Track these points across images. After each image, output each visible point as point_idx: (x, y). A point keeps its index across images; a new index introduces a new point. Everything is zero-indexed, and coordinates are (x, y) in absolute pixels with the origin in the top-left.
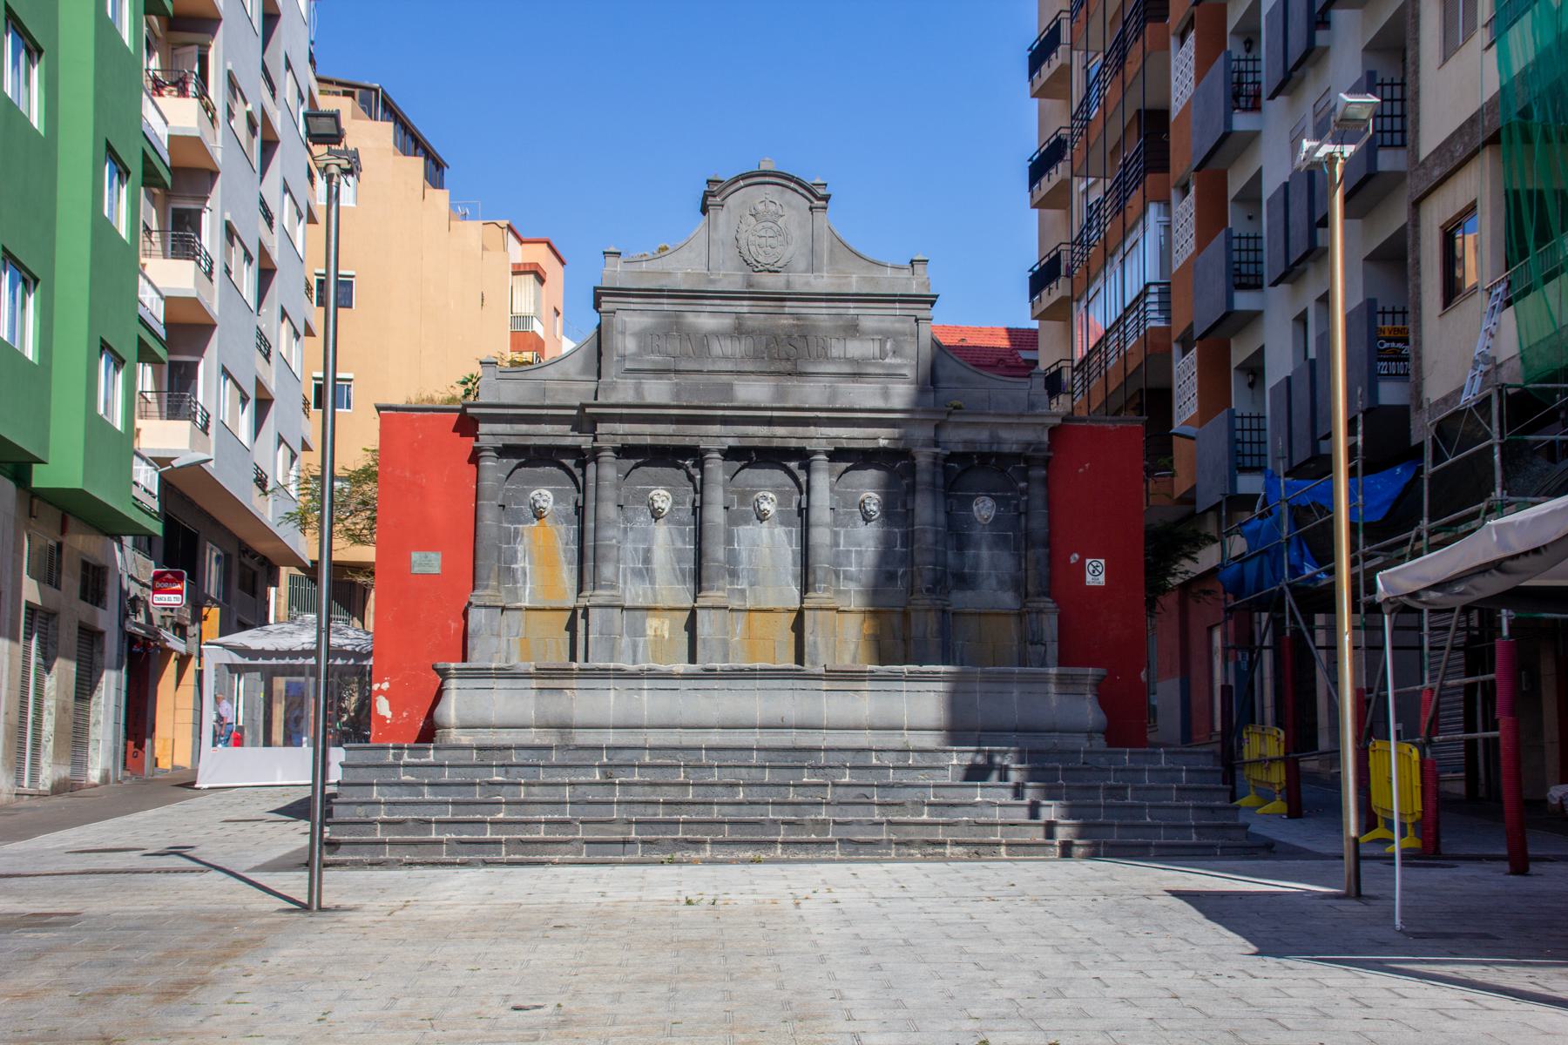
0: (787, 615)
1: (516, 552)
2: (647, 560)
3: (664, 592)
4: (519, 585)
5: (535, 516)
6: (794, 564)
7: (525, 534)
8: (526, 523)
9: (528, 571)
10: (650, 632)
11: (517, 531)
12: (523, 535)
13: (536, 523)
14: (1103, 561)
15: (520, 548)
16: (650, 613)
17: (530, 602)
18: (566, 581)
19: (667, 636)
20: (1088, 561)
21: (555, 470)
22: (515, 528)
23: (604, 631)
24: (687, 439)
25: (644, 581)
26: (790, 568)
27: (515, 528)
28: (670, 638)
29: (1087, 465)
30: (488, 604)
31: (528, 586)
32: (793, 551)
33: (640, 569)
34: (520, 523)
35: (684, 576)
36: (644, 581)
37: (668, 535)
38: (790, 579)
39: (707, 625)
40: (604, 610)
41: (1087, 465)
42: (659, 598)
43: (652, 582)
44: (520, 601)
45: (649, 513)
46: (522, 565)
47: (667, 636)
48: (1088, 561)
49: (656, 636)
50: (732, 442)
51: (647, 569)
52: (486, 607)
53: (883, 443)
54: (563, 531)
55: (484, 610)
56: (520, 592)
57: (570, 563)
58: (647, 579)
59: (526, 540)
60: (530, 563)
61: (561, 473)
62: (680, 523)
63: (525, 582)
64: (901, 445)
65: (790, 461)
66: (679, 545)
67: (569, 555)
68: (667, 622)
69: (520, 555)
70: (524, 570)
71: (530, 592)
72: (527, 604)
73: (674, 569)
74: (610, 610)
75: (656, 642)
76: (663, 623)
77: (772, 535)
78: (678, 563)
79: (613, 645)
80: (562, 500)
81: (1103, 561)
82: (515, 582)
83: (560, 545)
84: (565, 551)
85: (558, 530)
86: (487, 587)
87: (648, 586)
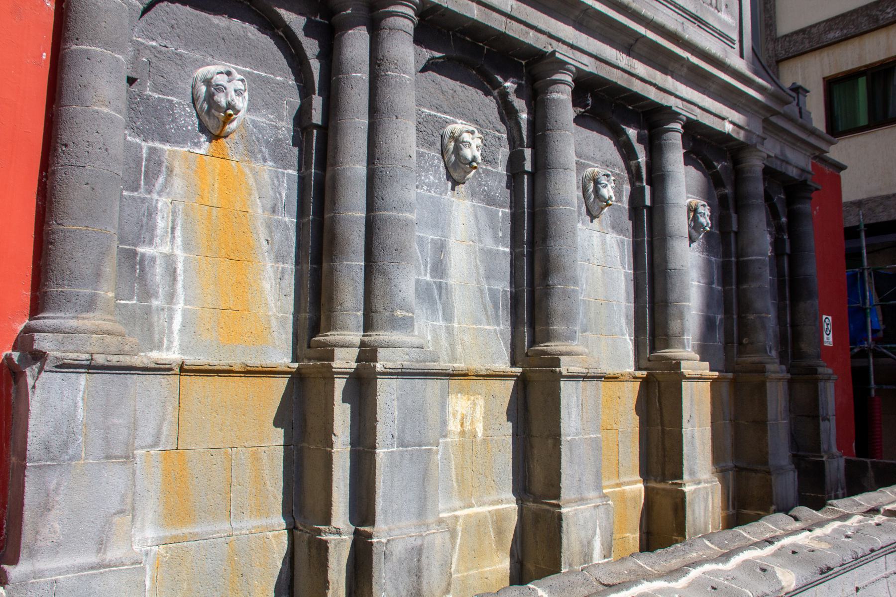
0: (630, 384)
1: (151, 213)
2: (439, 268)
3: (466, 339)
4: (155, 303)
5: (203, 129)
6: (628, 300)
7: (177, 170)
8: (177, 143)
9: (180, 270)
10: (454, 426)
11: (155, 162)
12: (170, 170)
13: (205, 147)
14: (830, 318)
15: (162, 203)
16: (454, 383)
17: (183, 350)
18: (271, 299)
19: (480, 434)
20: (824, 317)
21: (251, 31)
22: (152, 150)
23: (408, 438)
24: (532, 33)
25: (434, 312)
26: (624, 303)
27: (152, 150)
28: (485, 436)
29: (818, 208)
30: (100, 359)
31: (180, 306)
32: (626, 275)
33: (427, 283)
34: (165, 139)
35: (496, 307)
36: (434, 312)
37: (472, 218)
38: (623, 321)
39: (574, 411)
40: (407, 383)
41: (818, 208)
42: (459, 349)
43: (448, 317)
44: (159, 348)
45: (442, 170)
46: (166, 249)
47: (480, 434)
48: (824, 317)
49: (463, 433)
50: (590, 66)
51: (440, 287)
52: (91, 368)
53: (728, 128)
54: (266, 176)
55: (82, 380)
56: (159, 321)
57: (279, 257)
58: (440, 307)
59: (178, 184)
60: (187, 246)
61: (266, 42)
62: (490, 200)
63: (171, 296)
64: (741, 136)
65: (629, 126)
66: (489, 243)
67: (277, 237)
68: (481, 402)
69: (161, 224)
70: (170, 260)
71: (184, 325)
72: (172, 355)
73: (481, 291)
74: (418, 383)
75: (462, 446)
76: (474, 404)
77: (604, 243)
78: (488, 278)
79: (426, 470)
80: (267, 105)
81: (830, 318)
82: (147, 293)
83: (259, 211)
84: (269, 226)
85: (255, 174)
86: (91, 305)
87: (442, 323)
